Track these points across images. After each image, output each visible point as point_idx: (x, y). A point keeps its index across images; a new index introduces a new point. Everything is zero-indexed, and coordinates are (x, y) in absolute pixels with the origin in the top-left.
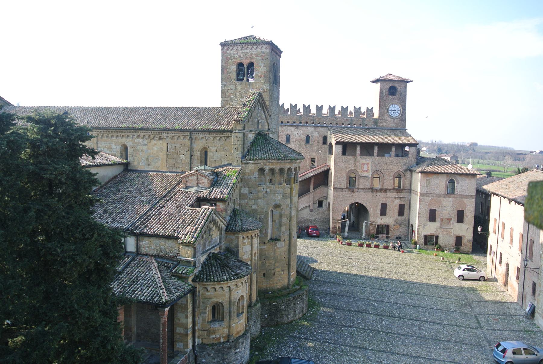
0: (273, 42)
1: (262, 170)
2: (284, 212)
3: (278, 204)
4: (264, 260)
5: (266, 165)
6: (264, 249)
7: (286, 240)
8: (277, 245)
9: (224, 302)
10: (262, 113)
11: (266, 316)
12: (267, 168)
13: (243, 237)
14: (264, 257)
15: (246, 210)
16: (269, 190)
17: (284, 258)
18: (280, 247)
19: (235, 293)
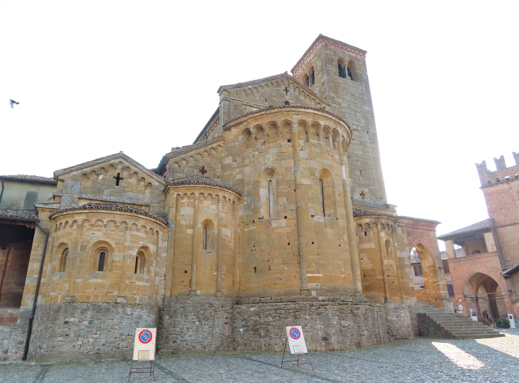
0: (323, 35)
1: (248, 132)
2: (282, 177)
4: (254, 246)
5: (249, 123)
6: (253, 230)
7: (288, 217)
9: (69, 242)
10: (302, 98)
11: (241, 330)
12: (252, 127)
13: (178, 195)
14: (253, 242)
15: (230, 183)
16: (256, 153)
17: (289, 244)
18: (278, 228)
19: (87, 233)
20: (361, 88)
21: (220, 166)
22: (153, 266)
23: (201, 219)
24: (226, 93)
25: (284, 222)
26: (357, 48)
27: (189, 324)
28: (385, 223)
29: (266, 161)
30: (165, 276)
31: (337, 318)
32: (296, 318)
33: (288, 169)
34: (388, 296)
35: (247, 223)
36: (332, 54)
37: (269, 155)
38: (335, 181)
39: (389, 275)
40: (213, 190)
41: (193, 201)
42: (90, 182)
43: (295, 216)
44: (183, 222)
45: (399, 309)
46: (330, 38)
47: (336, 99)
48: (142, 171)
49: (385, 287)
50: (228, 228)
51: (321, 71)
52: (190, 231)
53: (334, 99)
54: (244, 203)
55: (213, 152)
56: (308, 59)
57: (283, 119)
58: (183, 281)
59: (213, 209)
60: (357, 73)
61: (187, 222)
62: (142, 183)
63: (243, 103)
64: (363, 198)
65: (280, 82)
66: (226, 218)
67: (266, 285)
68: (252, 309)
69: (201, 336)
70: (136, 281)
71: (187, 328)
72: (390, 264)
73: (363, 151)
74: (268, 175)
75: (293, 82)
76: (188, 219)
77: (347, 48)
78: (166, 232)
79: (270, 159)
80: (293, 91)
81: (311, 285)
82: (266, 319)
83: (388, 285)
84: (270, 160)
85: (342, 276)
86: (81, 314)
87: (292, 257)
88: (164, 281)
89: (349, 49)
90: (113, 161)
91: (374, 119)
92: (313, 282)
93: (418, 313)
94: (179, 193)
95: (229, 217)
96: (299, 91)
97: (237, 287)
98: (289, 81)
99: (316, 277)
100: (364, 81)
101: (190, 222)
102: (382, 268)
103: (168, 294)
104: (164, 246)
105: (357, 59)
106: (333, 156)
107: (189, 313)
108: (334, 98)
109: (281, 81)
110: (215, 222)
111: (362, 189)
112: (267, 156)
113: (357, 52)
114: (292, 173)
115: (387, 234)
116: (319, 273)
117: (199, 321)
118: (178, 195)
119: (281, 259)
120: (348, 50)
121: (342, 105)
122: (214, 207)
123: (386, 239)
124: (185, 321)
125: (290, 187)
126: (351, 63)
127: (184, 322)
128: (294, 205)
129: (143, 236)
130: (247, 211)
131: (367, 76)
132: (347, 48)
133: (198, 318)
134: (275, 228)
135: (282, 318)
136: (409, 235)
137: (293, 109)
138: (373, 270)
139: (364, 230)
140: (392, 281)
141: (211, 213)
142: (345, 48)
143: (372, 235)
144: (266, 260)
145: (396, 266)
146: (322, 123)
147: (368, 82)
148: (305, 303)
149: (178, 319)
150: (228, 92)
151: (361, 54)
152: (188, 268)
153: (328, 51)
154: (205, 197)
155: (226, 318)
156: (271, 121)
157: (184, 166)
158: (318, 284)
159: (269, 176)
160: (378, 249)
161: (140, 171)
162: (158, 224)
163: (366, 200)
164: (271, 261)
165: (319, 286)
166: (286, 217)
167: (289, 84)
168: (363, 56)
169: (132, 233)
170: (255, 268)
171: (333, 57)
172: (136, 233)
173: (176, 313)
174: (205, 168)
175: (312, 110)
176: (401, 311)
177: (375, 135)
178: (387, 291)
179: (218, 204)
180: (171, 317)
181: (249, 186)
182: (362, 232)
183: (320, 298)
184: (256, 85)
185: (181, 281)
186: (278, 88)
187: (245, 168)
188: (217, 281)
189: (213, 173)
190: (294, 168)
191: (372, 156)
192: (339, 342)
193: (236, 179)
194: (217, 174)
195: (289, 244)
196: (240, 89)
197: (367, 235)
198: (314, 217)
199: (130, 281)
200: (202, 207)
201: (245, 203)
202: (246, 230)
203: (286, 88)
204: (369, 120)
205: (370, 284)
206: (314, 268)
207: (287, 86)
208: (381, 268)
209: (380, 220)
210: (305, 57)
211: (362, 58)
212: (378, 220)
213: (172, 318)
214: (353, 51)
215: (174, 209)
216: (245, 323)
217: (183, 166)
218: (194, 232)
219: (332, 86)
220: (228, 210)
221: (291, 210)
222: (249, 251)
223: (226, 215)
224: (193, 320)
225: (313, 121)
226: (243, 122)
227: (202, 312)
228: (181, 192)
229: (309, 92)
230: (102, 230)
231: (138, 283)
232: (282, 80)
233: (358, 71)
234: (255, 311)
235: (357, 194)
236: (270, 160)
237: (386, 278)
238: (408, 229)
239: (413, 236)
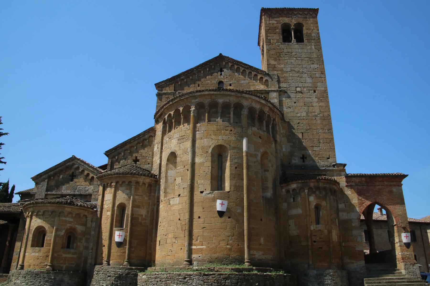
17: (179, 220)
22: (82, 242)
25: (177, 200)
26: (305, 9)
30: (92, 249)
42: (54, 182)
50: (143, 208)
64: (304, 161)
66: (141, 200)
70: (63, 254)
72: (318, 229)
77: (294, 12)
86: (22, 278)
89: (295, 13)
90: (69, 164)
104: (93, 226)
115: (318, 197)
120: (295, 14)
123: (315, 203)
129: (69, 220)
137: (190, 94)
139: (292, 196)
142: (290, 13)
158: (200, 255)
164: (167, 235)
169: (61, 219)
172: (64, 219)
174: (138, 157)
175: (207, 92)
195: (179, 220)
197: (295, 201)
199: (58, 254)
214: (301, 13)
221: (184, 188)
223: (139, 197)
225: (210, 101)
230: (41, 218)
231: (64, 255)
235: (296, 158)
239: (367, 195)
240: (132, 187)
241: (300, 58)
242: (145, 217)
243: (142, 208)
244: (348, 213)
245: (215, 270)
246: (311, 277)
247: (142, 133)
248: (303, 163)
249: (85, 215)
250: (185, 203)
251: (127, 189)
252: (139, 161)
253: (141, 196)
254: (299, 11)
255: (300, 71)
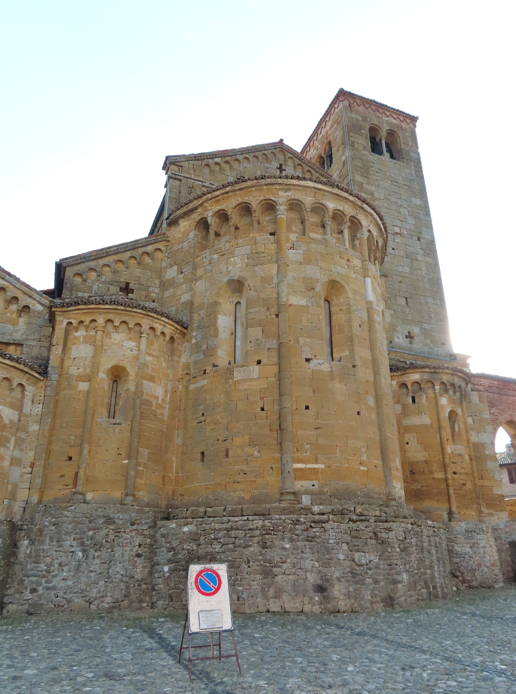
0: (345, 89)
1: (204, 224)
2: (254, 294)
3: (236, 278)
4: (203, 415)
6: (203, 387)
7: (264, 361)
8: (235, 374)
11: (166, 569)
13: (70, 323)
14: (202, 407)
15: (171, 309)
16: (216, 256)
17: (262, 409)
18: (245, 380)
20: (408, 171)
21: (157, 282)
22: (8, 448)
23: (106, 364)
24: (176, 168)
25: (255, 371)
26: (401, 112)
27: (64, 557)
28: (449, 382)
29: (230, 268)
30: (32, 466)
31: (345, 547)
32: (264, 547)
33: (266, 280)
34: (454, 509)
35: (195, 375)
36: (361, 119)
37: (236, 258)
38: (352, 303)
39: (457, 471)
40: (130, 315)
41: (94, 333)
43: (275, 359)
44: (74, 371)
45: (474, 532)
46: (356, 95)
47: (365, 186)
48: (14, 286)
49: (448, 492)
50: (159, 382)
51: (342, 144)
52: (83, 386)
53: (362, 186)
54: (191, 341)
55: (147, 259)
56: (324, 132)
57: (262, 198)
58: (64, 476)
59: (128, 348)
60: (401, 149)
61: (81, 370)
62: (14, 307)
63: (204, 184)
64: (411, 343)
65: (270, 156)
66: (156, 365)
67: (219, 484)
68: (186, 529)
69: (84, 579)
71: (60, 565)
72: (457, 452)
73: (410, 267)
74: (233, 292)
75: (292, 156)
76: (82, 364)
77: (386, 112)
78: (42, 388)
79: (237, 264)
80: (292, 170)
81: (300, 485)
82: (210, 549)
83: (454, 489)
84: (237, 266)
85: (362, 468)
87: (268, 432)
88: (30, 476)
89: (388, 113)
91: (430, 218)
92: (305, 480)
93: (511, 540)
94: (70, 321)
95: (161, 364)
96: (303, 172)
97: (169, 489)
98: (285, 155)
99: (311, 469)
100: (414, 161)
101: (85, 369)
102: (443, 458)
103: (35, 499)
104: (36, 411)
105: (401, 128)
106: (350, 260)
107: (65, 534)
108: (362, 183)
109: (272, 155)
110: (132, 371)
111: (409, 328)
112: (232, 259)
113: (402, 118)
114: (274, 285)
115: (452, 401)
116: (316, 462)
117: (84, 551)
118: (70, 323)
119: (247, 437)
120: (386, 115)
121: (376, 195)
122: (132, 344)
123: (449, 410)
124: (56, 551)
125: (268, 309)
126: (391, 133)
127: (54, 553)
128: (275, 341)
130: (195, 355)
131: (418, 154)
132: (386, 112)
133: (82, 544)
134: (239, 382)
135: (239, 546)
136: (492, 404)
138: (426, 462)
140: (462, 482)
141: (124, 355)
143: (425, 402)
144: (221, 438)
145: (470, 456)
146: (331, 205)
147: (420, 162)
148: (283, 517)
149: (45, 547)
150: (179, 166)
151: (408, 121)
152: (73, 452)
153: (353, 114)
154: (116, 327)
155: (140, 545)
156: (241, 202)
157: (92, 280)
159: (236, 295)
160: (436, 425)
161: (11, 286)
162: (22, 371)
163: (415, 346)
164: (229, 441)
165: (316, 486)
166: (259, 362)
167: (285, 160)
168: (411, 124)
170: (203, 454)
171: (361, 123)
173: (41, 535)
174: (130, 285)
176: (478, 536)
177: (432, 242)
178: (453, 500)
179: (140, 340)
180: (32, 542)
181: (201, 312)
182: (407, 397)
183: (316, 509)
184: (229, 158)
185: (61, 475)
186: (266, 165)
187: (197, 284)
188: (127, 476)
189: (144, 293)
190: (278, 278)
191: (426, 276)
192: (348, 595)
193: (182, 301)
194: (152, 295)
195: (262, 409)
196: (200, 162)
197: (416, 402)
198: (311, 361)
200: (108, 344)
201: (194, 341)
202: (192, 387)
203: (281, 165)
204: (420, 219)
205: (421, 486)
206: (308, 453)
207: (282, 162)
208: (442, 460)
209: (439, 376)
210: (319, 129)
211: (410, 127)
212: (435, 376)
213: (33, 544)
214: (395, 116)
215: (60, 348)
216: (173, 556)
217: (90, 281)
218: (90, 387)
219: (358, 166)
220: (159, 351)
221: (269, 349)
222: (195, 423)
223: (154, 360)
224: (73, 549)
226: (196, 208)
227: (91, 533)
228: (74, 319)
229: (319, 173)
232: (273, 153)
233: (403, 146)
234: (190, 532)
235: (400, 336)
236: (237, 266)
237: (450, 476)
238: (489, 394)
239: (500, 407)
240: (142, 335)
241: (396, 184)
242: (162, 402)
243: (157, 384)
244: (478, 433)
245: (356, 512)
246: (459, 534)
247: (141, 239)
248: (410, 346)
249: (21, 385)
250: (274, 379)
251: (130, 339)
252: (132, 293)
253: (157, 357)
254: (394, 113)
255: (398, 203)
